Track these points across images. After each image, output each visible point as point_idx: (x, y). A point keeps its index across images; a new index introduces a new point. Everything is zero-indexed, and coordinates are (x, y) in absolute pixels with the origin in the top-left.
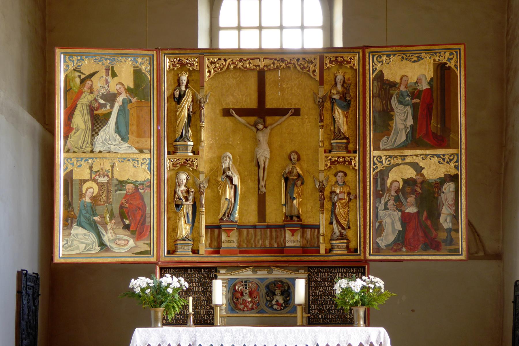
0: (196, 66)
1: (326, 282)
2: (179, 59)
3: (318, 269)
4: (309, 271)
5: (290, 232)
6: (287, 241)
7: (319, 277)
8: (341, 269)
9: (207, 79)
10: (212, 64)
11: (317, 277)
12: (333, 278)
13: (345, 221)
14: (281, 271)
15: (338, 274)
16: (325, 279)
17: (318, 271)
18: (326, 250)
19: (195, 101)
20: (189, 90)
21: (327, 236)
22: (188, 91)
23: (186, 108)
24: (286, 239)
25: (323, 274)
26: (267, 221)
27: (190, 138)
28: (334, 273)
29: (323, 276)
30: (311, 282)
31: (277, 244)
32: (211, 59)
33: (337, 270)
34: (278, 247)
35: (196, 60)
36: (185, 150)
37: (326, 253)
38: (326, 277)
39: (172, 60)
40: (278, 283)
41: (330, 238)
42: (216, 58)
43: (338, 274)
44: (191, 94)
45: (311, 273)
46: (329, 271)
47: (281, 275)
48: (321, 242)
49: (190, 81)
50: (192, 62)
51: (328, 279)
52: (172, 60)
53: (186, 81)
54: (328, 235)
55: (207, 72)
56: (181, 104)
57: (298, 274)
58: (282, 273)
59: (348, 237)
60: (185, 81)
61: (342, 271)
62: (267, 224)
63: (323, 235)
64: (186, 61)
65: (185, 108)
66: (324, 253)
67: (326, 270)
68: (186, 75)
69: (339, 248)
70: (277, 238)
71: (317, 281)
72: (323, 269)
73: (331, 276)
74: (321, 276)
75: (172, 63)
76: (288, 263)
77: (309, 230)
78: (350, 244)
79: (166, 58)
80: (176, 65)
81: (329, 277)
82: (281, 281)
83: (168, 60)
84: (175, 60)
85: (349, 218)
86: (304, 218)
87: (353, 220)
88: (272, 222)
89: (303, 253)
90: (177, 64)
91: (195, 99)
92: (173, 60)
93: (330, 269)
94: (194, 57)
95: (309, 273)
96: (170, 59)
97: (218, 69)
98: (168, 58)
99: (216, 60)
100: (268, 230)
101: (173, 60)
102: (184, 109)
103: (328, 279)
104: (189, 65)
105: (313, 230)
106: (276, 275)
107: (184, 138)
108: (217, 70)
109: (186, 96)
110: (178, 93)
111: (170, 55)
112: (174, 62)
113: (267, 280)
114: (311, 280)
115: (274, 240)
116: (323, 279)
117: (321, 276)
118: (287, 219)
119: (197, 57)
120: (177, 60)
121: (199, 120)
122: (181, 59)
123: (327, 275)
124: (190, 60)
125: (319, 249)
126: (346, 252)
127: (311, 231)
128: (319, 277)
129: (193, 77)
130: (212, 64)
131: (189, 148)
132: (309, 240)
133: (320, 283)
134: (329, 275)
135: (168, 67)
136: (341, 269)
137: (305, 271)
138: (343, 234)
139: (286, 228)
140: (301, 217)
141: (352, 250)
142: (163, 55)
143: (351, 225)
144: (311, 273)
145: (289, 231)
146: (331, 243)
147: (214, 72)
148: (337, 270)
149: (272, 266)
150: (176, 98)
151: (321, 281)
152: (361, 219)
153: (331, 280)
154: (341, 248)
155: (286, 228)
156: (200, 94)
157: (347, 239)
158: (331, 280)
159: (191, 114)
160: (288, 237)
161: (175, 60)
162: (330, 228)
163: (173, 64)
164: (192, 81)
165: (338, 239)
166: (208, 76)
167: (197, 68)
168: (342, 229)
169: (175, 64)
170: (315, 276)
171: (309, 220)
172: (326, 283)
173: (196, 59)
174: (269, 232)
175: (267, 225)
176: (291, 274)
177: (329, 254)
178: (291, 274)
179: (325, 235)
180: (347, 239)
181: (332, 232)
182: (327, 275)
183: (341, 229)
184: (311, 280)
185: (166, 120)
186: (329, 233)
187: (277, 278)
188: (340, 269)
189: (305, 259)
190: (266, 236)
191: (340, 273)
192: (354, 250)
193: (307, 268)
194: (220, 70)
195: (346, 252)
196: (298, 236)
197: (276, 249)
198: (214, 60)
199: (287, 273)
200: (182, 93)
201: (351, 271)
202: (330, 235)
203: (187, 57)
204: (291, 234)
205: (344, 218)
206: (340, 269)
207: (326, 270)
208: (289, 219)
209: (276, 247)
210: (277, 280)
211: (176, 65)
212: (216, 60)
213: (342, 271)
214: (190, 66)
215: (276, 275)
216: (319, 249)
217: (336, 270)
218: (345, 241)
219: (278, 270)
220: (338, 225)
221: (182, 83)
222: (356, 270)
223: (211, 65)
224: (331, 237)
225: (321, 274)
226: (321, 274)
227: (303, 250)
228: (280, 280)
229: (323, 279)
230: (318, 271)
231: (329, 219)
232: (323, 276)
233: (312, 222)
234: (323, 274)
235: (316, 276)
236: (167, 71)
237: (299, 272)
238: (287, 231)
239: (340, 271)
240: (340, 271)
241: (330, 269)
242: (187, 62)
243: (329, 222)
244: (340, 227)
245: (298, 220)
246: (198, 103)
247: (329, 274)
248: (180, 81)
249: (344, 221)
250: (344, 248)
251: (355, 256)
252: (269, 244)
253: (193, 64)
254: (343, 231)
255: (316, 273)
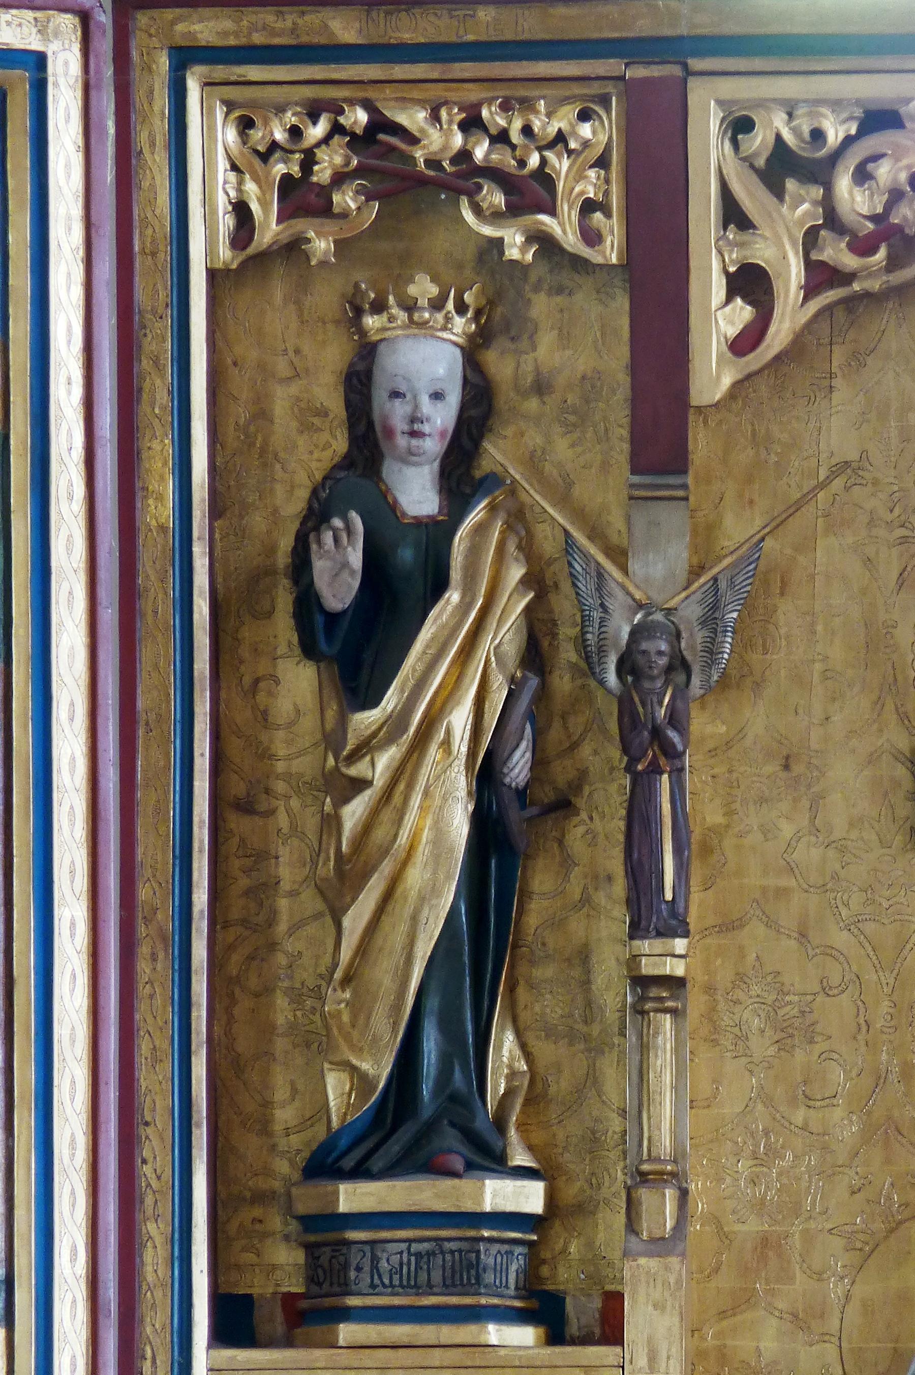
0: (589, 207)
2: (362, 116)
9: (727, 381)
10: (791, 185)
19: (568, 654)
20: (492, 509)
22: (481, 529)
23: (460, 745)
27: (500, 1124)
32: (779, 121)
35: (586, 130)
36: (449, 1287)
39: (280, 135)
42: (836, 104)
44: (516, 572)
49: (505, 396)
50: (534, 160)
52: (280, 135)
53: (454, 399)
55: (718, 288)
56: (391, 700)
60: (437, 396)
64: (458, 140)
65: (447, 744)
68: (459, 323)
75: (279, 169)
79: (207, 112)
80: (325, 192)
83: (231, 135)
84: (317, 131)
90: (340, 179)
91: (567, 631)
92: (295, 132)
94: (551, 91)
96: (246, 125)
97: (863, 247)
98: (230, 105)
99: (834, 134)
101: (295, 132)
102: (433, 752)
104: (498, 199)
107: (430, 1128)
108: (850, 261)
109: (453, 596)
110: (356, 558)
111: (254, 72)
112: (309, 161)
119: (596, 89)
120: (337, 129)
121: (620, 888)
122: (401, 119)
124: (501, 138)
129: (546, 341)
130: (791, 185)
131: (489, 1257)
135: (226, 222)
142: (163, 62)
147: (810, 290)
150: (332, 618)
156: (634, 566)
159: (514, 815)
161: (317, 131)
163: (287, 184)
164: (532, 404)
166: (732, 331)
167: (592, 237)
169: (322, 173)
173: (584, 116)
185: (201, 898)
194: (893, 264)
198: (818, 135)
200: (406, 555)
203: (473, 94)
211: (325, 192)
212: (834, 134)
214: (515, 210)
221: (399, 424)
223: (779, 193)
236: (212, 275)
242: (464, 155)
246: (612, 678)
248: (379, 396)
253: (544, 177)
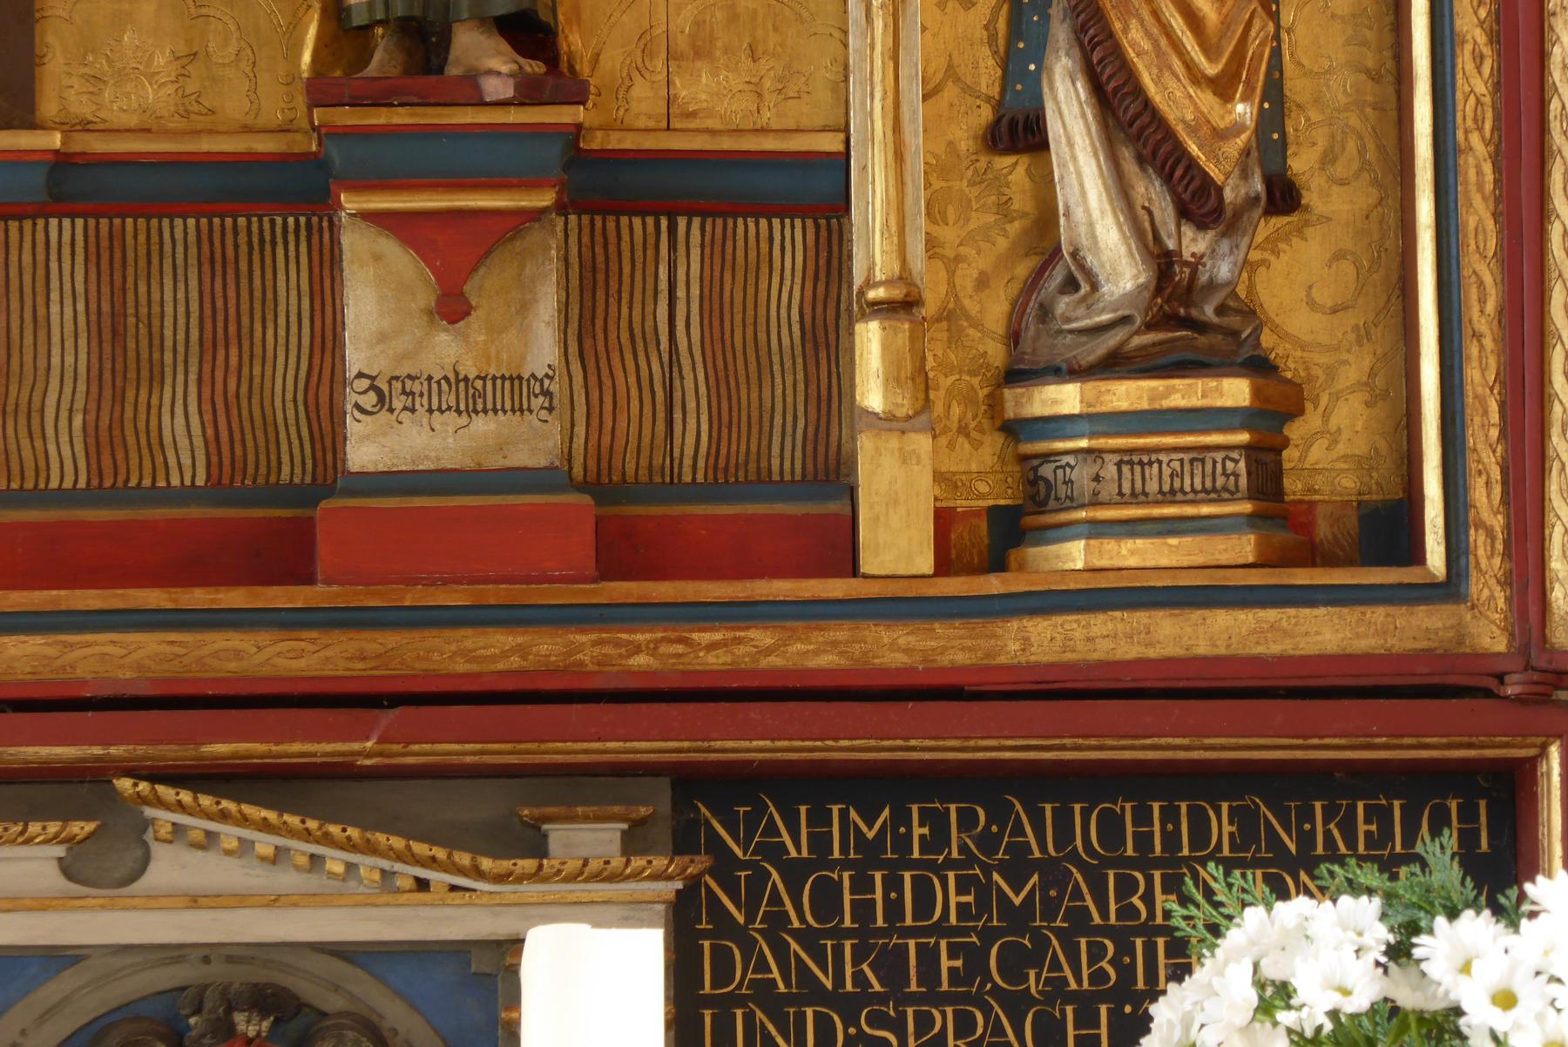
1: (941, 1000)
3: (820, 818)
4: (683, 843)
5: (399, 257)
6: (356, 395)
7: (839, 934)
8: (1170, 815)
11: (808, 938)
12: (1042, 943)
13: (1223, 87)
14: (265, 844)
15: (1126, 887)
16: (929, 958)
17: (820, 843)
18: (944, 520)
21: (950, 316)
24: (356, 358)
25: (893, 883)
26: (48, 108)
28: (1053, 873)
29: (894, 909)
30: (723, 1006)
31: (213, 444)
33: (1111, 829)
34: (218, 490)
37: (945, 565)
38: (941, 929)
40: (230, 1030)
41: (996, 354)
43: (1126, 887)
45: (724, 867)
46: (988, 842)
47: (275, 901)
48: (872, 395)
51: (975, 961)
54: (972, 307)
57: (531, 890)
58: (286, 880)
59: (1267, 339)
61: (1172, 840)
62: (56, 140)
63: (903, 306)
66: (925, 564)
67: (937, 821)
69: (1139, 497)
70: (210, 346)
71: (811, 991)
72: (902, 817)
73: (1017, 918)
74: (863, 910)
76: (388, 718)
77: (692, 231)
78: (1294, 431)
81: (988, 936)
82: (269, 1000)
85: (1277, 53)
86: (613, 60)
87: (1342, 87)
88: (133, 121)
89: (608, 570)
93: (999, 813)
95: (698, 864)
100: (64, 231)
103: (975, 961)
105: (745, 228)
106: (194, 901)
113: (68, 981)
114: (723, 972)
115: (156, 378)
116: (891, 966)
117: (863, 910)
118: (364, 58)
123: (950, 898)
125: (836, 507)
126: (1244, 547)
127: (716, 253)
128: (839, 934)
132: (693, 381)
133: (850, 1019)
134: (983, 904)
136: (1170, 815)
137: (632, 843)
138: (1191, 292)
139: (350, 203)
140: (573, 41)
141: (1323, 530)
143: (1300, 163)
144: (724, 867)
145: (390, 247)
146: (1015, 429)
148: (1111, 829)
149: (130, 772)
151: (864, 996)
152: (1465, 61)
153: (1014, 965)
154: (1169, 497)
155: (350, 203)
157: (1259, 367)
158: (1014, 965)
160: (382, 338)
162: (1004, 210)
165: (1115, 365)
168: (1184, 213)
170: (777, 921)
171: (682, 90)
172: (944, 1018)
174: (93, 257)
175: (62, 162)
176: (422, 885)
177: (993, 584)
178: (422, 885)
179: (930, 309)
180: (1259, 367)
181: (1023, 269)
182: (950, 898)
183: (1165, 211)
184: (723, 972)
186: (982, 282)
187: (208, 952)
188: (1142, 817)
189: (641, 661)
190: (41, 323)
191: (1144, 861)
192: (1352, 521)
193: (657, 801)
195: (1244, 547)
196: (525, 307)
197: (195, 512)
199: (368, 866)
201: (1306, 840)
202: (995, 310)
204: (426, 296)
205: (1210, 51)
206: (1142, 817)
207: (937, 821)
208: (382, 59)
209: (188, 494)
210: (217, 972)
213: (1172, 840)
215: (194, 901)
216: (836, 507)
217: (1087, 831)
218: (1236, 391)
219: (230, 834)
220: (1127, 154)
222: (1380, 815)
224: (1014, 337)
225: (862, 884)
226: (862, 884)
227: (599, 522)
228: (260, 975)
229: (891, 966)
230: (820, 843)
231: (987, 74)
232: (894, 909)
233: (737, 108)
234: (893, 883)
235: (800, 914)
237: (539, 849)
238: (356, 242)
239: (1143, 841)
240: (1143, 841)
241: (999, 813)
243: (986, 114)
244: (1151, 192)
245: (535, 67)
247: (984, 891)
249: (1207, 100)
250: (1213, 494)
251: (1378, 614)
252: (94, 449)
254: (1193, 243)
255: (794, 874)
